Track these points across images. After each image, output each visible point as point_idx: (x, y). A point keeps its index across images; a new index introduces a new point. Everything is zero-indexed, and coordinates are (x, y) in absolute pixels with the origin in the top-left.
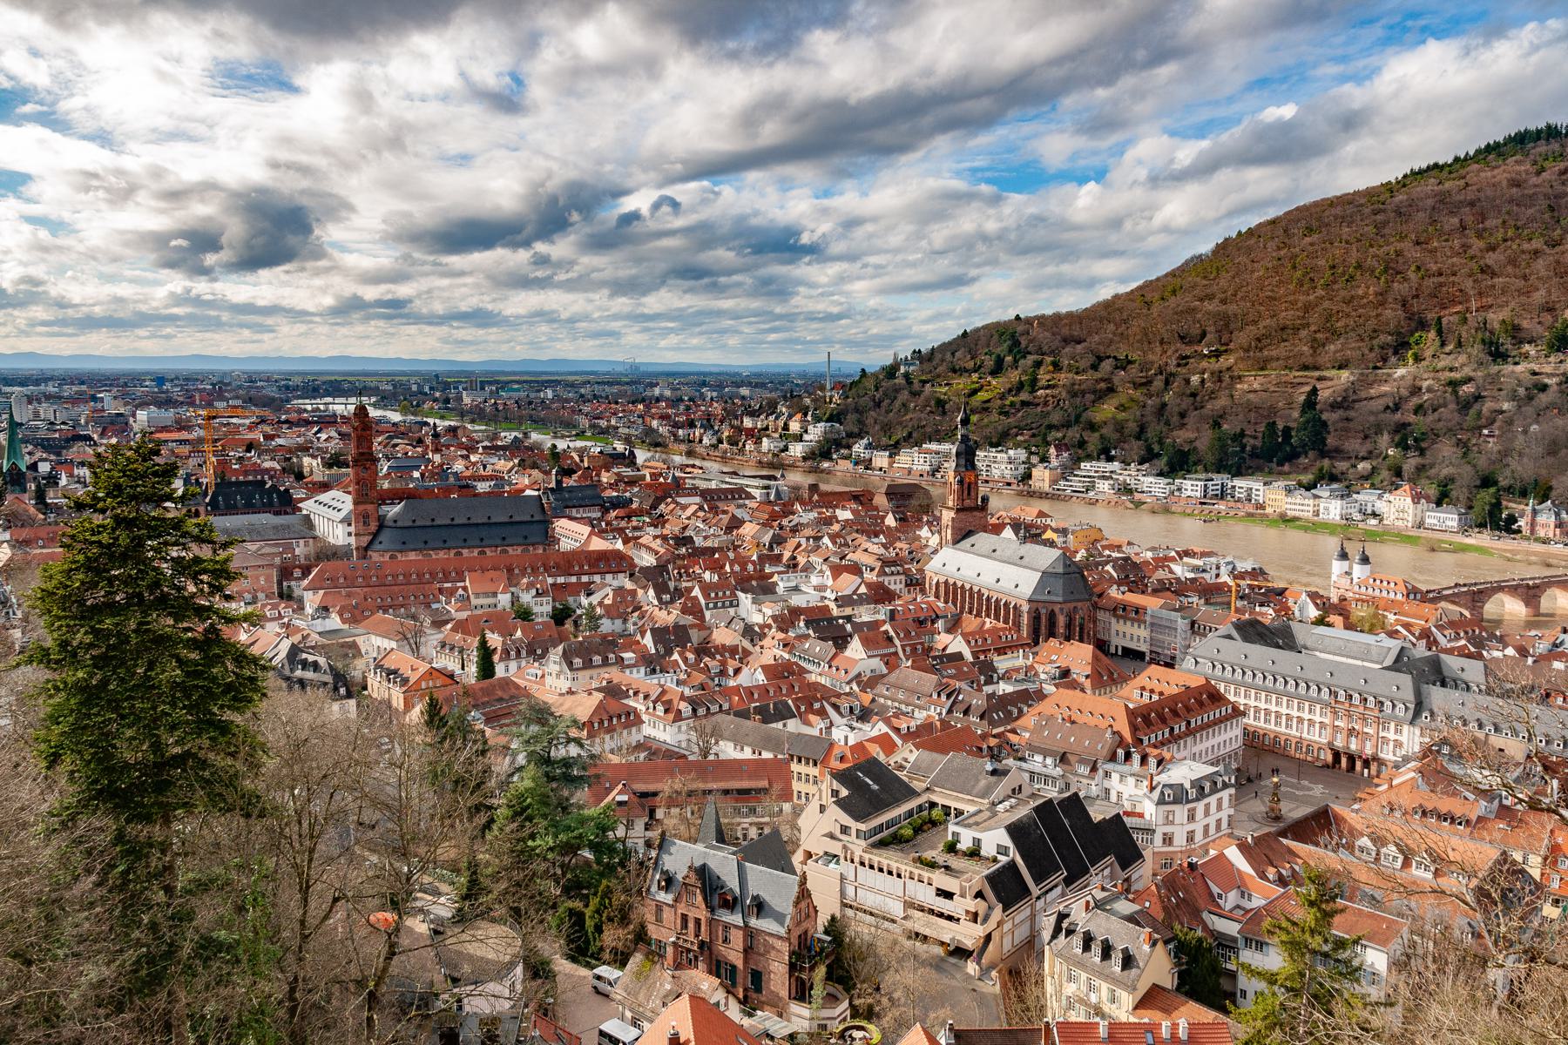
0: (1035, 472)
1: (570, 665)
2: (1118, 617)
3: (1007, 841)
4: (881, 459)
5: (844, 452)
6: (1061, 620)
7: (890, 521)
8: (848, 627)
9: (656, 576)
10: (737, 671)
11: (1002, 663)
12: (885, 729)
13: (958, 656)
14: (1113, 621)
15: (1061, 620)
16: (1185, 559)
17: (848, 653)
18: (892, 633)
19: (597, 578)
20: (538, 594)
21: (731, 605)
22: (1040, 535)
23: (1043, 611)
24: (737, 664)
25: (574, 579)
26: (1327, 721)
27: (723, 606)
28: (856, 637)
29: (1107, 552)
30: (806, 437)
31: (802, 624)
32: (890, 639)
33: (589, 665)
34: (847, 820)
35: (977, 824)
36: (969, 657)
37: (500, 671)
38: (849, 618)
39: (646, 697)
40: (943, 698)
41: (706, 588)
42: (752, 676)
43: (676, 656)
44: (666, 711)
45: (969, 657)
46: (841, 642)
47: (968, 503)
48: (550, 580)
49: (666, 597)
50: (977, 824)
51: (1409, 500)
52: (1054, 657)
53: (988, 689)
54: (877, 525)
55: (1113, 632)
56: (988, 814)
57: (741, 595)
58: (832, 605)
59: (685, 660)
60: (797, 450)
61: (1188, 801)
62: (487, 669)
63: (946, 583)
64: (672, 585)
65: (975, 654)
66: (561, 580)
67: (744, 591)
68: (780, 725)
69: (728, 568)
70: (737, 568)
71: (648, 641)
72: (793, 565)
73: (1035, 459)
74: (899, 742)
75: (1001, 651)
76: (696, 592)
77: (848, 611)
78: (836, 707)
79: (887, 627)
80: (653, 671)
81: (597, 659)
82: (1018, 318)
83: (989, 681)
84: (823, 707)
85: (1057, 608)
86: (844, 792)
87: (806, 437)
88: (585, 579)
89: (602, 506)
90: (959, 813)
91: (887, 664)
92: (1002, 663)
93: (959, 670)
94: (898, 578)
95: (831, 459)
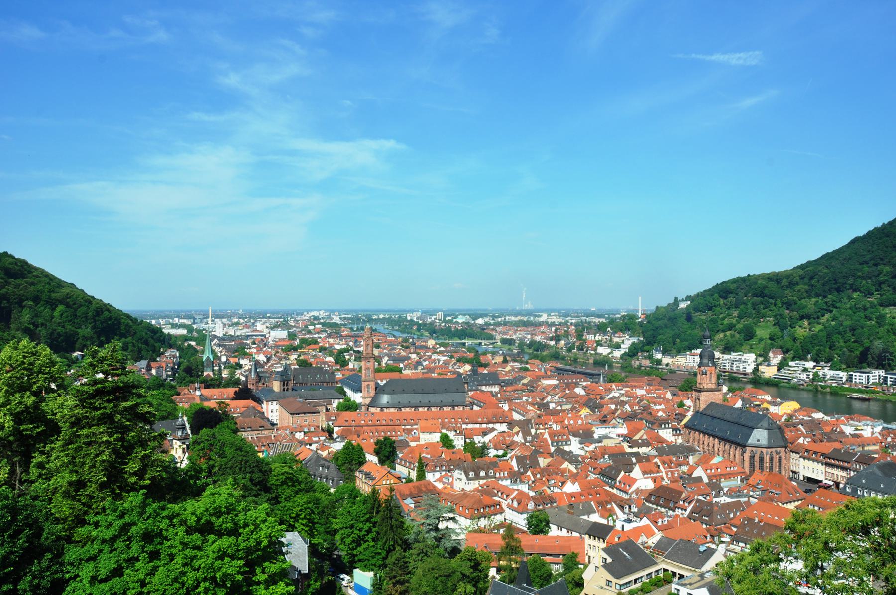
0: (760, 368)
1: (467, 474)
6: (767, 459)
7: (668, 396)
8: (634, 460)
9: (525, 426)
10: (563, 483)
11: (726, 484)
12: (648, 522)
13: (700, 479)
15: (767, 459)
16: (851, 422)
17: (632, 475)
18: (659, 463)
19: (491, 426)
20: (457, 435)
21: (567, 444)
24: (563, 479)
25: (478, 426)
28: (637, 465)
29: (801, 417)
31: (606, 456)
32: (658, 466)
33: (477, 477)
34: (611, 578)
35: (691, 584)
36: (706, 480)
37: (429, 476)
38: (636, 454)
39: (507, 496)
40: (687, 505)
41: (552, 434)
42: (572, 487)
43: (529, 473)
44: (519, 504)
45: (706, 480)
46: (629, 469)
48: (464, 426)
49: (529, 438)
50: (691, 584)
53: (718, 500)
54: (660, 398)
55: (802, 467)
56: (699, 578)
57: (571, 437)
58: (625, 445)
59: (534, 475)
60: (617, 354)
62: (421, 476)
64: (533, 431)
65: (709, 477)
66: (470, 426)
67: (574, 436)
68: (586, 517)
69: (567, 422)
70: (572, 422)
71: (514, 463)
72: (604, 421)
73: (760, 359)
74: (656, 531)
75: (728, 476)
76: (546, 436)
77: (635, 450)
78: (622, 508)
79: (656, 460)
80: (515, 481)
81: (483, 473)
83: (717, 496)
84: (612, 507)
86: (609, 560)
87: (622, 346)
88: (484, 426)
89: (500, 384)
90: (682, 576)
91: (655, 481)
92: (726, 484)
93: (699, 488)
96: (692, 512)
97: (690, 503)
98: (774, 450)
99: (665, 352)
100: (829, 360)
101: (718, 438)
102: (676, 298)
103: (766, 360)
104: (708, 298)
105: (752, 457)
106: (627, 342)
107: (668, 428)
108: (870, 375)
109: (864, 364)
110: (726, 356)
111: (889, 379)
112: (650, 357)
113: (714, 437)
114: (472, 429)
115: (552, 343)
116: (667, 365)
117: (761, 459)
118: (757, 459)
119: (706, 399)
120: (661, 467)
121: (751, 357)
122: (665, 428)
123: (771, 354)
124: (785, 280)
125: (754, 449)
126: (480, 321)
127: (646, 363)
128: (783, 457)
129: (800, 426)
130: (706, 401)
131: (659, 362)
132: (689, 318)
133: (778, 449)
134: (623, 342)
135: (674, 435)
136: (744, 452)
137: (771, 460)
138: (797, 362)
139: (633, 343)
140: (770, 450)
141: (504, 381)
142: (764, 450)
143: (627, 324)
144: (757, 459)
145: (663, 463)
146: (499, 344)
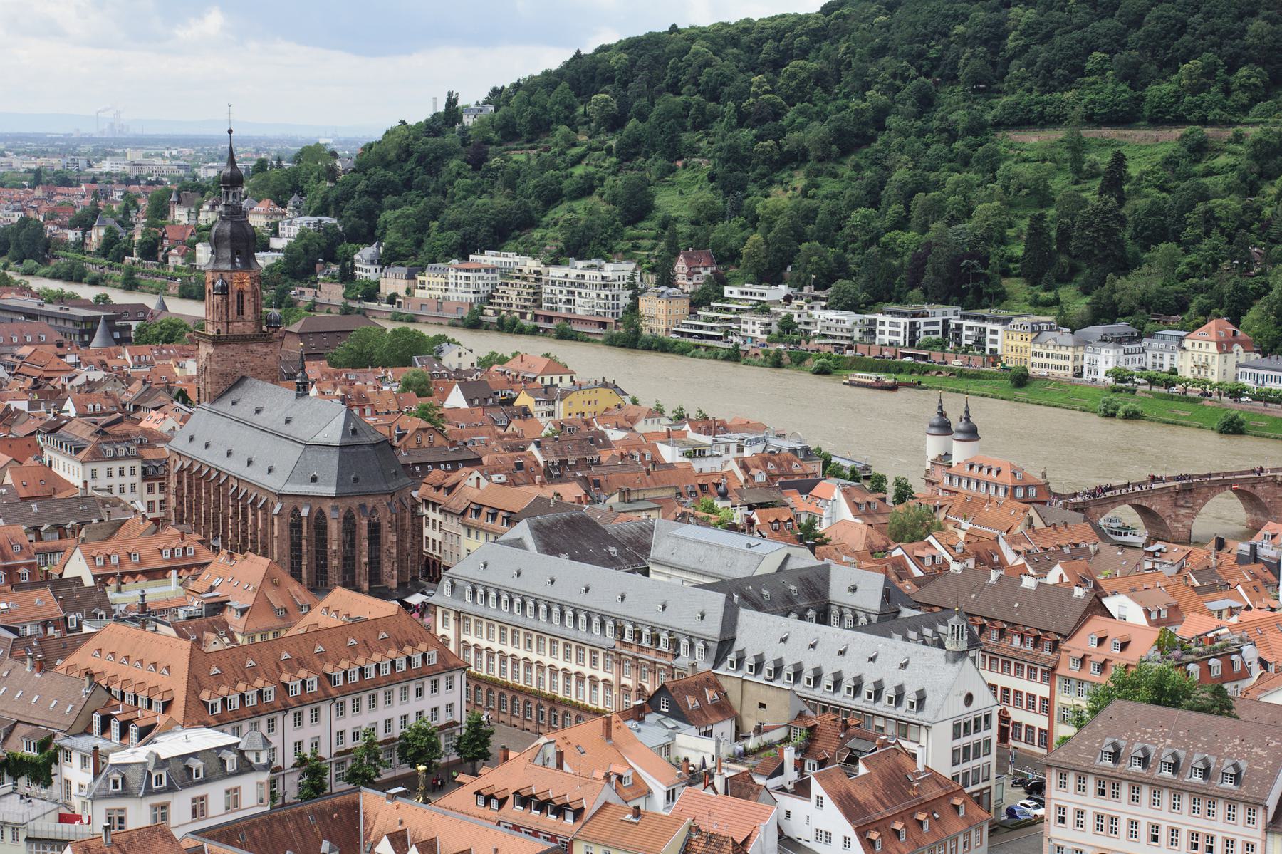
0: (645, 305)
2: (469, 528)
4: (394, 283)
5: (335, 268)
6: (334, 529)
14: (463, 532)
15: (334, 529)
22: (511, 401)
23: (305, 512)
26: (609, 677)
30: (276, 243)
47: (238, 328)
51: (1213, 347)
52: (216, 583)
61: (149, 792)
63: (189, 469)
85: (327, 508)
94: (127, 465)
95: (314, 284)
98: (355, 503)
102: (451, 102)
103: (667, 279)
104: (541, 94)
105: (296, 526)
106: (294, 227)
107: (127, 457)
108: (922, 320)
109: (916, 292)
110: (557, 272)
111: (965, 332)
112: (347, 277)
115: (71, 235)
116: (392, 299)
121: (618, 270)
122: (115, 458)
123: (681, 266)
124: (769, 45)
127: (333, 293)
128: (385, 525)
129: (532, 448)
130: (224, 375)
132: (478, 162)
133: (370, 502)
134: (276, 233)
135: (145, 477)
138: (748, 287)
139: (302, 235)
140: (344, 505)
143: (297, 176)
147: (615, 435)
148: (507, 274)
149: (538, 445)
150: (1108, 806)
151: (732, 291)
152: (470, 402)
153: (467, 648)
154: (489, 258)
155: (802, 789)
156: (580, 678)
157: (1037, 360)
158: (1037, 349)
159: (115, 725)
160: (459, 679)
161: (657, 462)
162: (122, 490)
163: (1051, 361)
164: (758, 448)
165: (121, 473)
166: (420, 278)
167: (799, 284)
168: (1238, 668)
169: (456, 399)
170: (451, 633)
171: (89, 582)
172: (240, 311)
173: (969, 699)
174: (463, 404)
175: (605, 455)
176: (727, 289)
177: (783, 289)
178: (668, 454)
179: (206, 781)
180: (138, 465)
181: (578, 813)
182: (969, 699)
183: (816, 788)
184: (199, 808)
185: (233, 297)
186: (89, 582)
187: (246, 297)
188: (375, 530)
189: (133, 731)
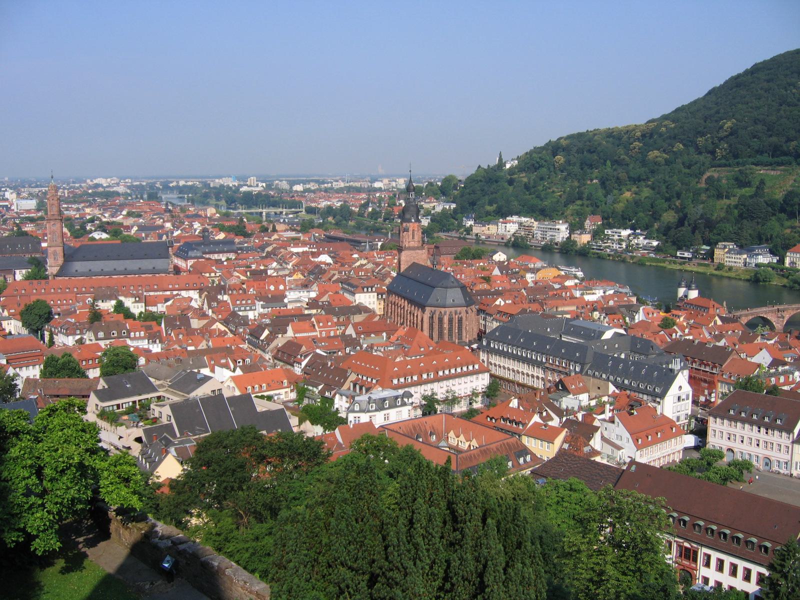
3: (170, 414)
4: (477, 229)
18: (315, 323)
21: (251, 310)
27: (245, 310)
32: (314, 326)
82: (588, 131)
96: (306, 366)
97: (306, 357)
98: (453, 309)
99: (479, 220)
100: (646, 227)
101: (407, 299)
102: (500, 159)
104: (534, 155)
105: (432, 318)
112: (460, 225)
113: (405, 298)
114: (156, 297)
117: (441, 320)
118: (436, 320)
119: (407, 259)
120: (316, 327)
122: (367, 291)
125: (433, 309)
126: (299, 188)
128: (464, 318)
130: (407, 261)
131: (469, 230)
133: (459, 309)
136: (423, 311)
137: (451, 321)
141: (241, 249)
142: (443, 310)
144: (436, 320)
145: (318, 322)
146: (304, 213)
147: (557, 286)
148: (520, 224)
149: (525, 289)
150: (732, 430)
151: (608, 232)
152: (502, 273)
153: (491, 364)
154: (515, 218)
155: (612, 421)
156: (533, 376)
157: (728, 260)
158: (728, 255)
159: (358, 387)
160: (486, 376)
161: (572, 297)
162: (370, 304)
163: (733, 260)
164: (611, 292)
165: (370, 297)
166: (487, 226)
167: (633, 228)
168: (791, 379)
169: (496, 272)
170: (485, 359)
171: (354, 336)
172: (413, 238)
173: (680, 387)
174: (499, 274)
175: (551, 293)
176: (606, 231)
177: (629, 232)
178: (578, 294)
179: (390, 407)
180: (376, 294)
181: (524, 425)
182: (680, 387)
183: (617, 420)
184: (386, 418)
185: (410, 232)
186: (354, 336)
187: (415, 233)
188: (460, 320)
189: (364, 389)
